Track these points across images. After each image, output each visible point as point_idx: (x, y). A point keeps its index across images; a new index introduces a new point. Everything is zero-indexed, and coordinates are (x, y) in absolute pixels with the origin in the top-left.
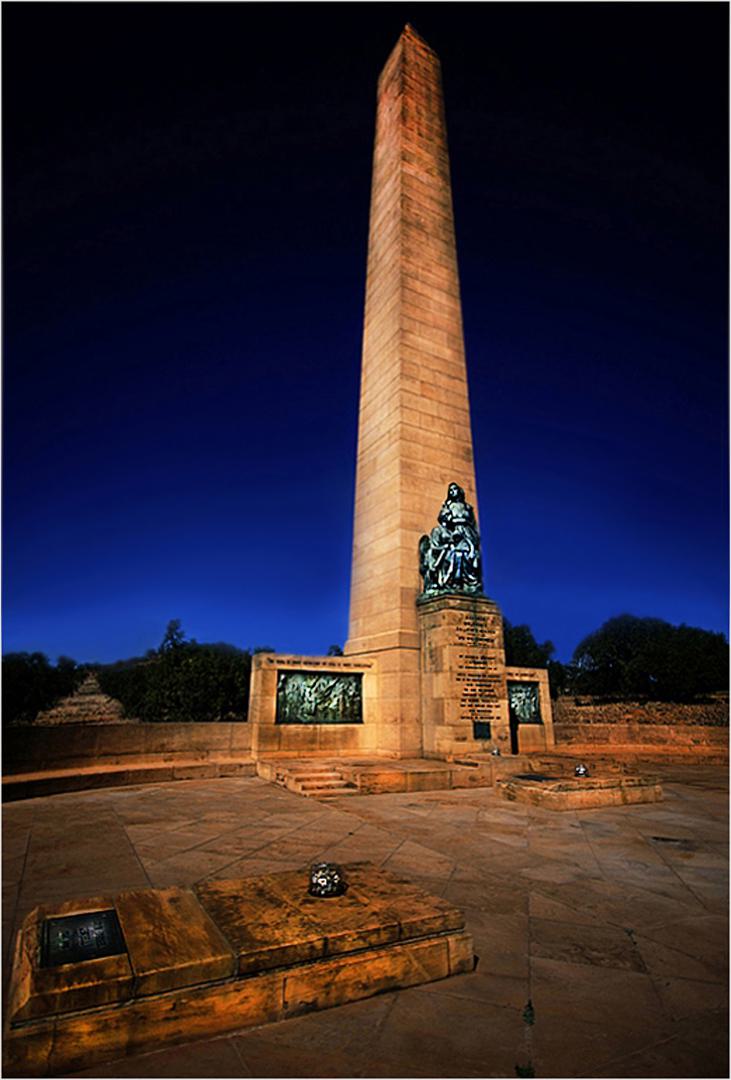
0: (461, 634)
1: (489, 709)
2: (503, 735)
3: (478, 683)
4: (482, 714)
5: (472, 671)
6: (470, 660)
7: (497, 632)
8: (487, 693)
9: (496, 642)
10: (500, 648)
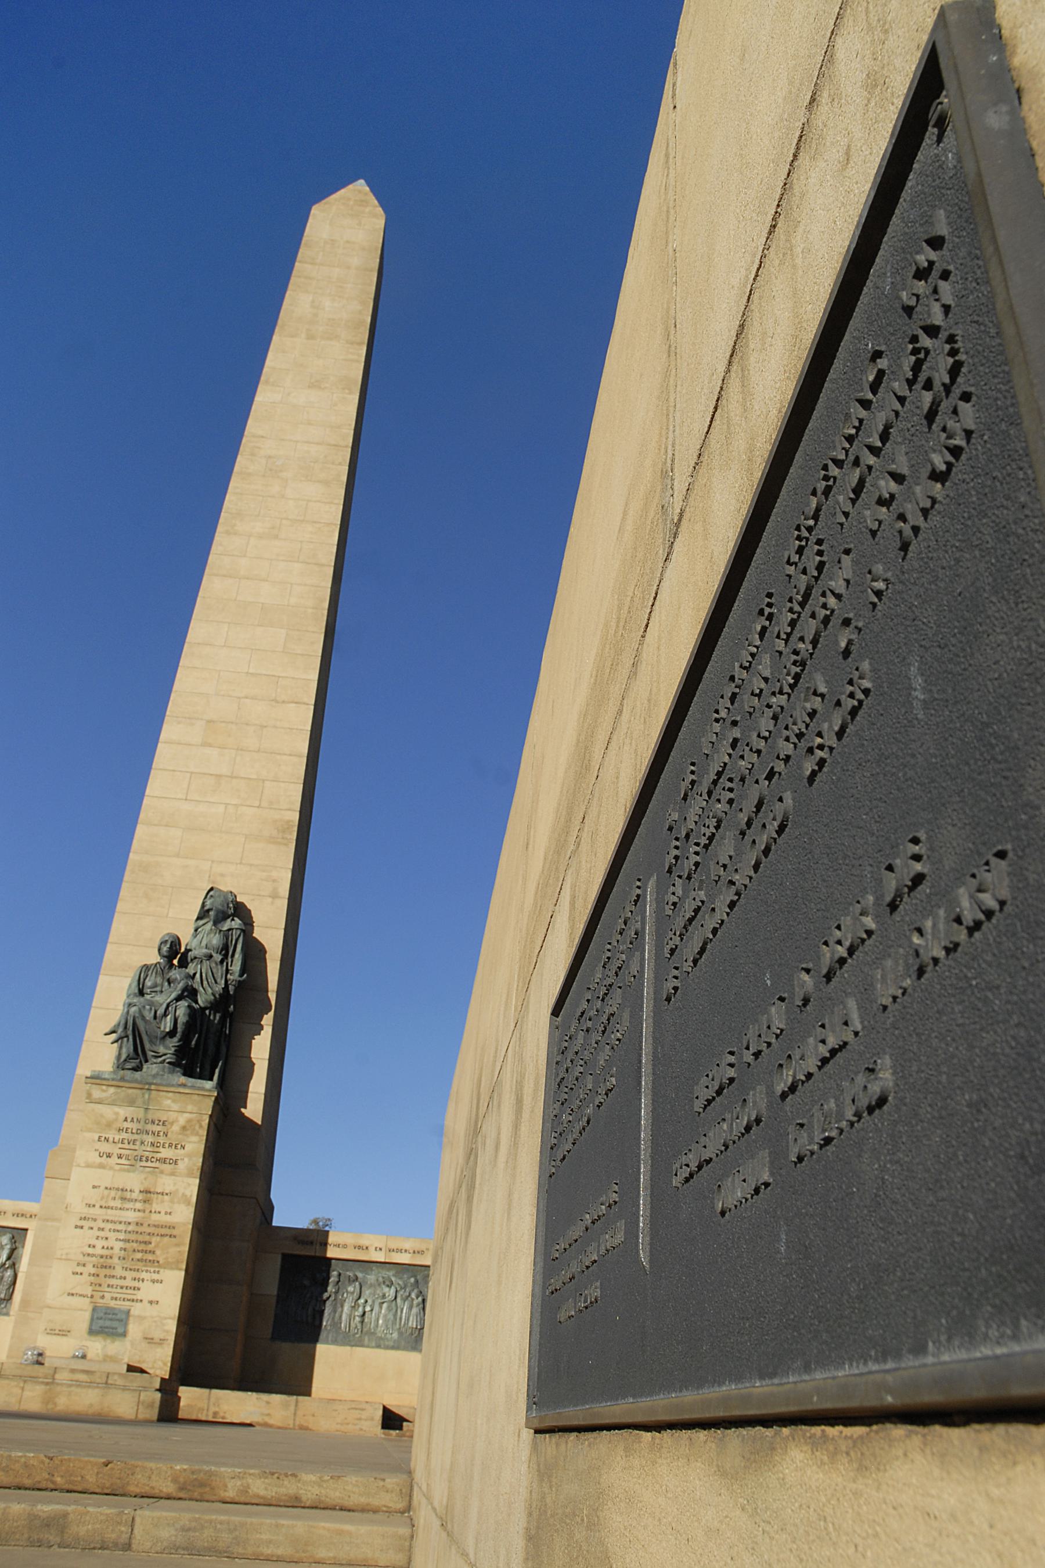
0: (106, 1147)
1: (136, 1284)
2: (157, 1335)
3: (122, 1236)
4: (116, 1292)
5: (111, 1214)
6: (113, 1193)
7: (189, 1147)
8: (139, 1256)
9: (181, 1165)
10: (190, 1174)
